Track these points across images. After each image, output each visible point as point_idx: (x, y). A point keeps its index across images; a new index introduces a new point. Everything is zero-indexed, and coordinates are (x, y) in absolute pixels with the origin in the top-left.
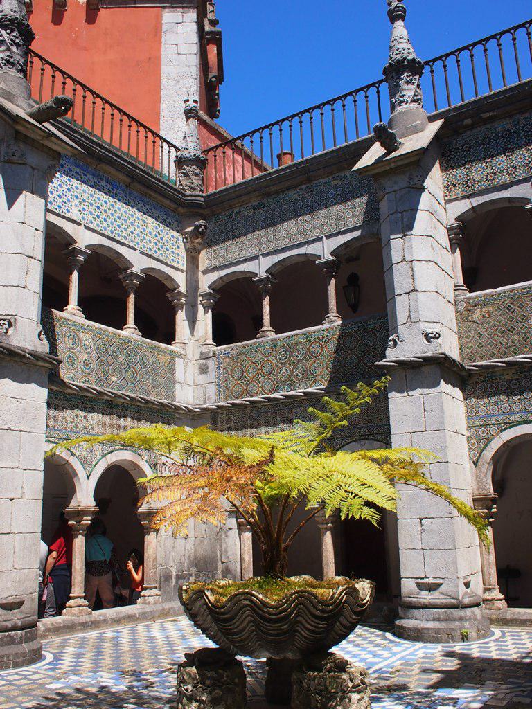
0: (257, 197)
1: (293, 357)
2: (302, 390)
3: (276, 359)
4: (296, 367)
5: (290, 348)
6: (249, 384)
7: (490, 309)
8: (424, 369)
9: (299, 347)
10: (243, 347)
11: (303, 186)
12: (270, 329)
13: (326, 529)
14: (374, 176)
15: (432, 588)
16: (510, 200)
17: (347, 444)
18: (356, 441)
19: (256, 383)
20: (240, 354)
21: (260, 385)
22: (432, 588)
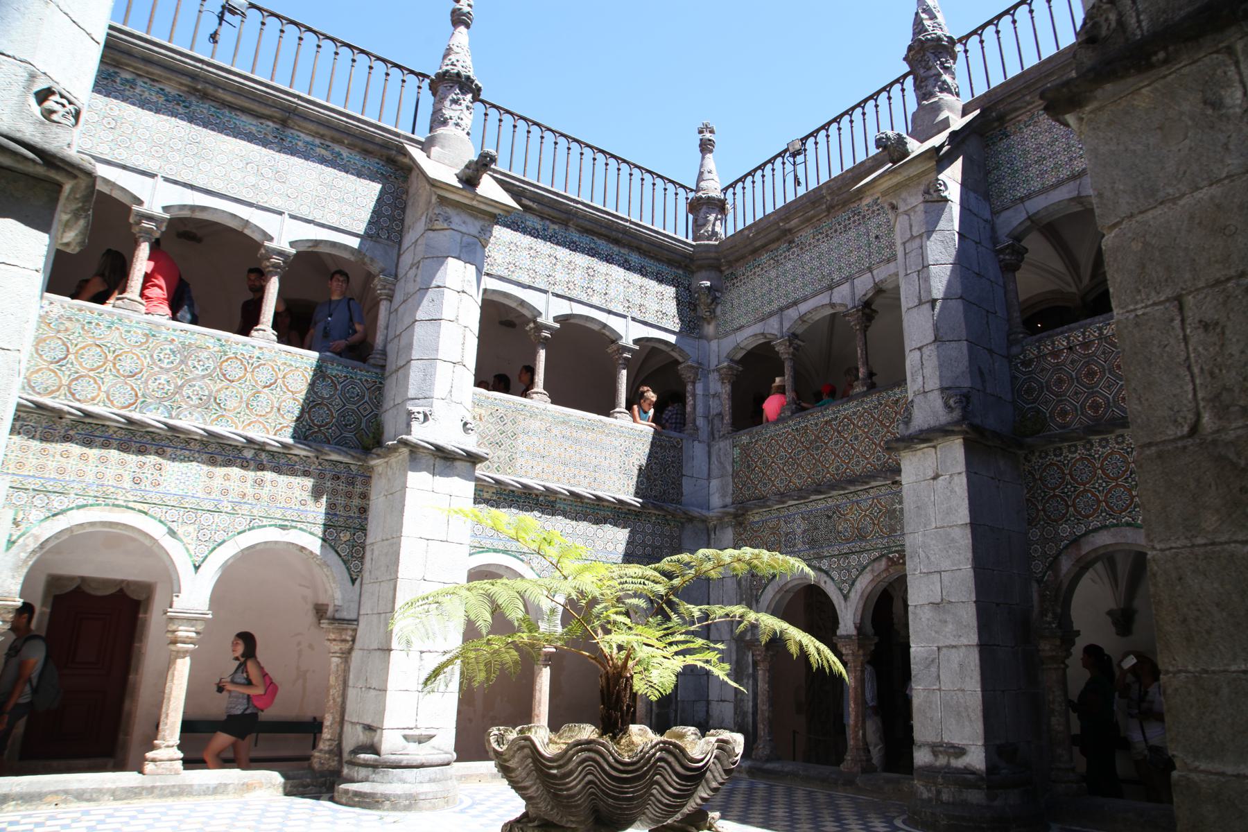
0: (181, 84)
1: (187, 365)
2: (202, 426)
3: (152, 356)
4: (189, 383)
5: (185, 352)
6: (76, 379)
7: (483, 412)
8: (458, 464)
9: (205, 354)
10: (80, 310)
11: (270, 124)
12: (139, 299)
13: (184, 654)
14: (439, 196)
15: (421, 740)
16: (522, 303)
17: (260, 527)
18: (275, 525)
19: (95, 382)
20: (69, 319)
21: (103, 388)
22: (421, 740)
